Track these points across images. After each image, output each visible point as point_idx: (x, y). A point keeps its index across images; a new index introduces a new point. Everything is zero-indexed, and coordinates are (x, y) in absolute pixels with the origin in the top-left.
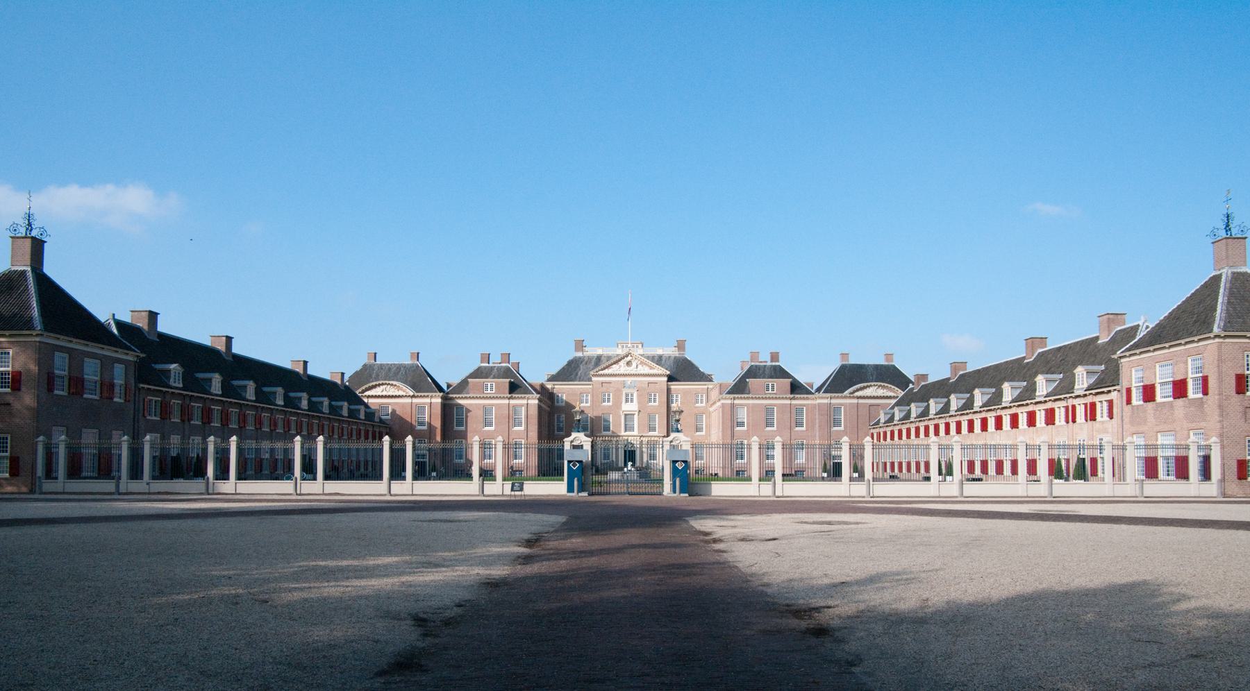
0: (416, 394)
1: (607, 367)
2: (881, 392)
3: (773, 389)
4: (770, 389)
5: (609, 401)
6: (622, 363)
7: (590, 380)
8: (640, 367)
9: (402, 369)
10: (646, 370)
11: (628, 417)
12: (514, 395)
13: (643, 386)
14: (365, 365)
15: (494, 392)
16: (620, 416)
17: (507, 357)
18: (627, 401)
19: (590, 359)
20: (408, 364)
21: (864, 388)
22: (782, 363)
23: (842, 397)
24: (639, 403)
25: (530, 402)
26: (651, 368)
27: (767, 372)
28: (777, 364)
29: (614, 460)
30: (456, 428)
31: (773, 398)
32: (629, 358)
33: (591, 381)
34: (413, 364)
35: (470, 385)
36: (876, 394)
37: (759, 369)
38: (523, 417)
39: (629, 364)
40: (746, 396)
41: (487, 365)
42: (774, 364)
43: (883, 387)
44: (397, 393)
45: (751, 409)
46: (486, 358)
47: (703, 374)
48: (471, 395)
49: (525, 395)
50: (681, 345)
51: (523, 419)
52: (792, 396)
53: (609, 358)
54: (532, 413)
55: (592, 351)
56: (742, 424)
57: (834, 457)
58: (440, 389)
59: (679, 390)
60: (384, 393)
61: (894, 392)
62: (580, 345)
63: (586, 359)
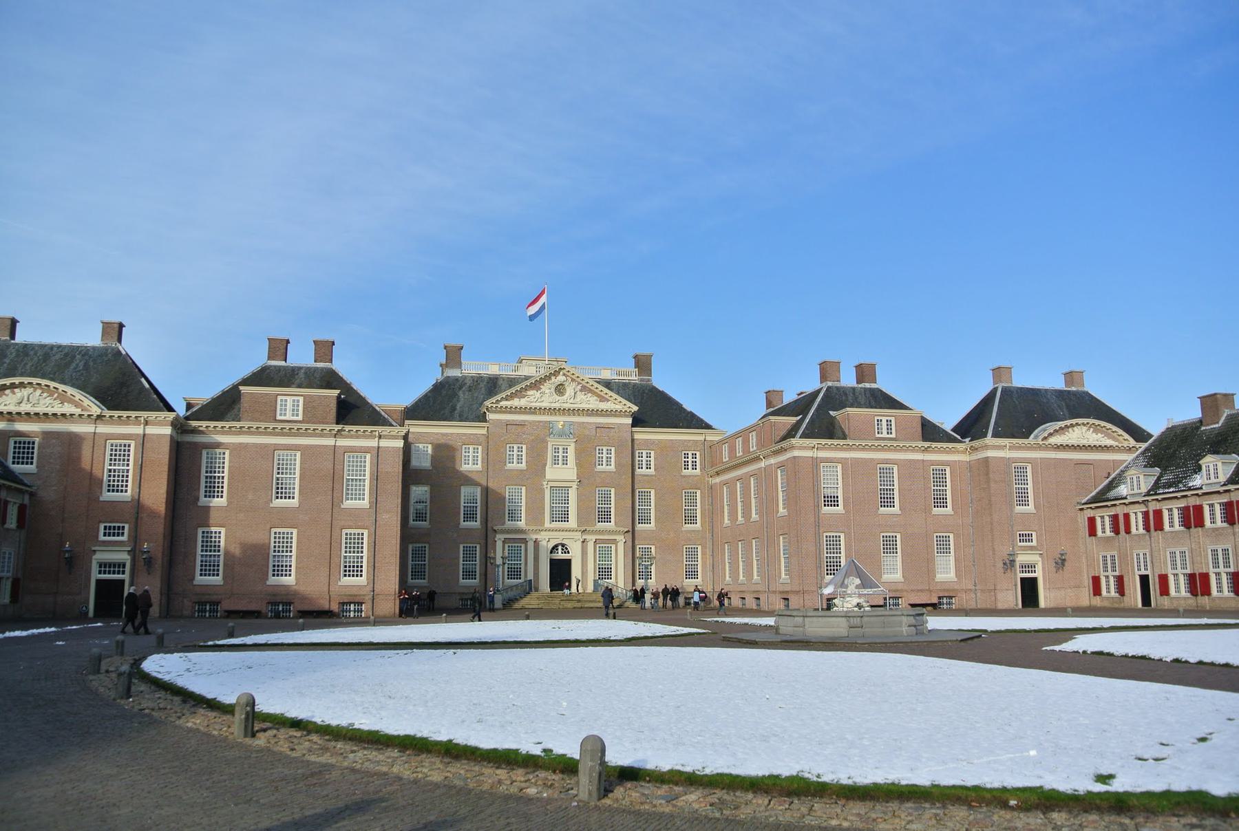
0: (108, 413)
1: (519, 394)
2: (1093, 438)
3: (889, 431)
4: (885, 431)
5: (519, 461)
6: (547, 388)
7: (482, 418)
8: (581, 396)
10: (592, 402)
11: (560, 491)
13: (587, 432)
15: (300, 418)
16: (542, 491)
17: (324, 349)
18: (555, 461)
19: (478, 380)
20: (94, 348)
22: (884, 383)
24: (579, 465)
25: (384, 443)
28: (874, 386)
30: (203, 501)
32: (561, 378)
33: (485, 421)
34: (106, 349)
35: (245, 403)
38: (368, 477)
39: (560, 389)
41: (282, 363)
42: (868, 385)
43: (1097, 429)
44: (58, 409)
46: (279, 347)
47: (692, 415)
50: (643, 364)
51: (367, 483)
52: (927, 444)
53: (512, 382)
55: (471, 367)
56: (832, 501)
59: (653, 442)
60: (25, 408)
61: (1114, 439)
62: (453, 355)
63: (468, 382)
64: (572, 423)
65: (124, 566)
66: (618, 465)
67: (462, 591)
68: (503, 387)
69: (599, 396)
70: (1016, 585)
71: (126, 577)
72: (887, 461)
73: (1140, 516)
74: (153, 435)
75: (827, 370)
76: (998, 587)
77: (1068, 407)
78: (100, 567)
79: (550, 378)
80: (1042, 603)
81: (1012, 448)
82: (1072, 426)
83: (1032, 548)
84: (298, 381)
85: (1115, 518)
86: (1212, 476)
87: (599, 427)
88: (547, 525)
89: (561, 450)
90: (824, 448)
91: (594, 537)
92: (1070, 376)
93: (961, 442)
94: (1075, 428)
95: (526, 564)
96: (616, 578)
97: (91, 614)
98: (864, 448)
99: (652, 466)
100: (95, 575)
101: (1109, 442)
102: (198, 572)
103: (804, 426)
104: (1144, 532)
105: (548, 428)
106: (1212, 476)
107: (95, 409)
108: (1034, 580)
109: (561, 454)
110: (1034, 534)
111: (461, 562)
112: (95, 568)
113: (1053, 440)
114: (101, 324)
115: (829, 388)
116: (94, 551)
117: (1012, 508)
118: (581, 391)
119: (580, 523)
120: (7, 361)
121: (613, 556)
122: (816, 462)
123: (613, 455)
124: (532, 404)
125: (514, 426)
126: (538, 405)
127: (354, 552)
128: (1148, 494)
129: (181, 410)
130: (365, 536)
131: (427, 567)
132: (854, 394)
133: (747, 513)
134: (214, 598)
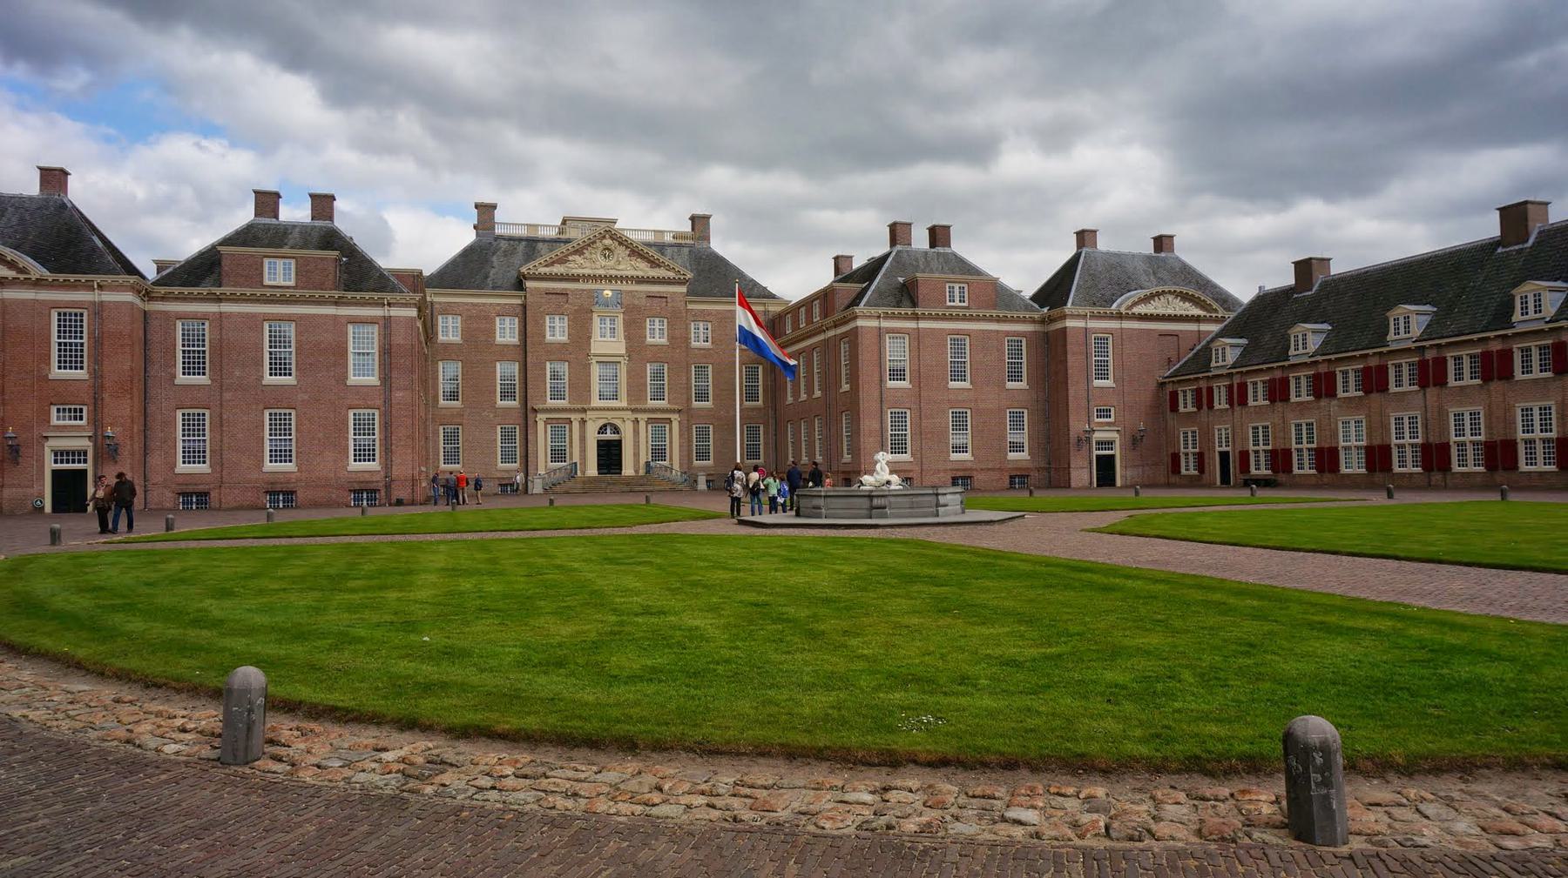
1: (562, 261)
4: (957, 299)
10: (643, 269)
12: (349, 295)
13: (636, 302)
15: (292, 283)
17: (323, 204)
20: (31, 199)
21: (1152, 297)
23: (1111, 317)
24: (628, 338)
25: (395, 312)
26: (654, 264)
28: (947, 250)
29: (576, 459)
30: (181, 379)
31: (965, 318)
36: (1170, 311)
40: (909, 311)
43: (1185, 297)
45: (917, 337)
46: (267, 201)
47: (755, 284)
48: (227, 290)
49: (380, 295)
57: (1102, 444)
58: (131, 269)
59: (709, 313)
65: (85, 453)
66: (671, 338)
67: (499, 475)
68: (543, 252)
69: (649, 261)
70: (1091, 463)
71: (89, 466)
72: (958, 332)
73: (1223, 390)
74: (110, 302)
75: (897, 233)
76: (1072, 466)
77: (1154, 273)
78: (56, 455)
79: (594, 242)
80: (1119, 483)
81: (1094, 317)
82: (1158, 294)
83: (1109, 424)
84: (291, 242)
85: (1198, 392)
86: (1300, 346)
88: (596, 402)
90: (887, 317)
91: (643, 417)
92: (1162, 243)
93: (1038, 311)
94: (1161, 297)
95: (571, 446)
96: (671, 459)
97: (48, 508)
98: (931, 318)
99: (710, 339)
100: (50, 465)
101: (1197, 312)
102: (180, 459)
103: (869, 293)
104: (1227, 406)
105: (594, 297)
106: (1300, 346)
107: (37, 270)
108: (1113, 457)
110: (1112, 409)
111: (499, 444)
112: (49, 458)
113: (1136, 310)
114: (39, 171)
115: (899, 252)
116: (46, 437)
117: (1088, 381)
118: (629, 255)
119: (629, 402)
121: (667, 436)
122: (880, 332)
123: (665, 327)
124: (574, 271)
125: (554, 296)
126: (580, 271)
127: (364, 434)
128: (1233, 367)
129: (151, 273)
130: (377, 417)
131: (461, 450)
133: (810, 391)
134: (201, 488)
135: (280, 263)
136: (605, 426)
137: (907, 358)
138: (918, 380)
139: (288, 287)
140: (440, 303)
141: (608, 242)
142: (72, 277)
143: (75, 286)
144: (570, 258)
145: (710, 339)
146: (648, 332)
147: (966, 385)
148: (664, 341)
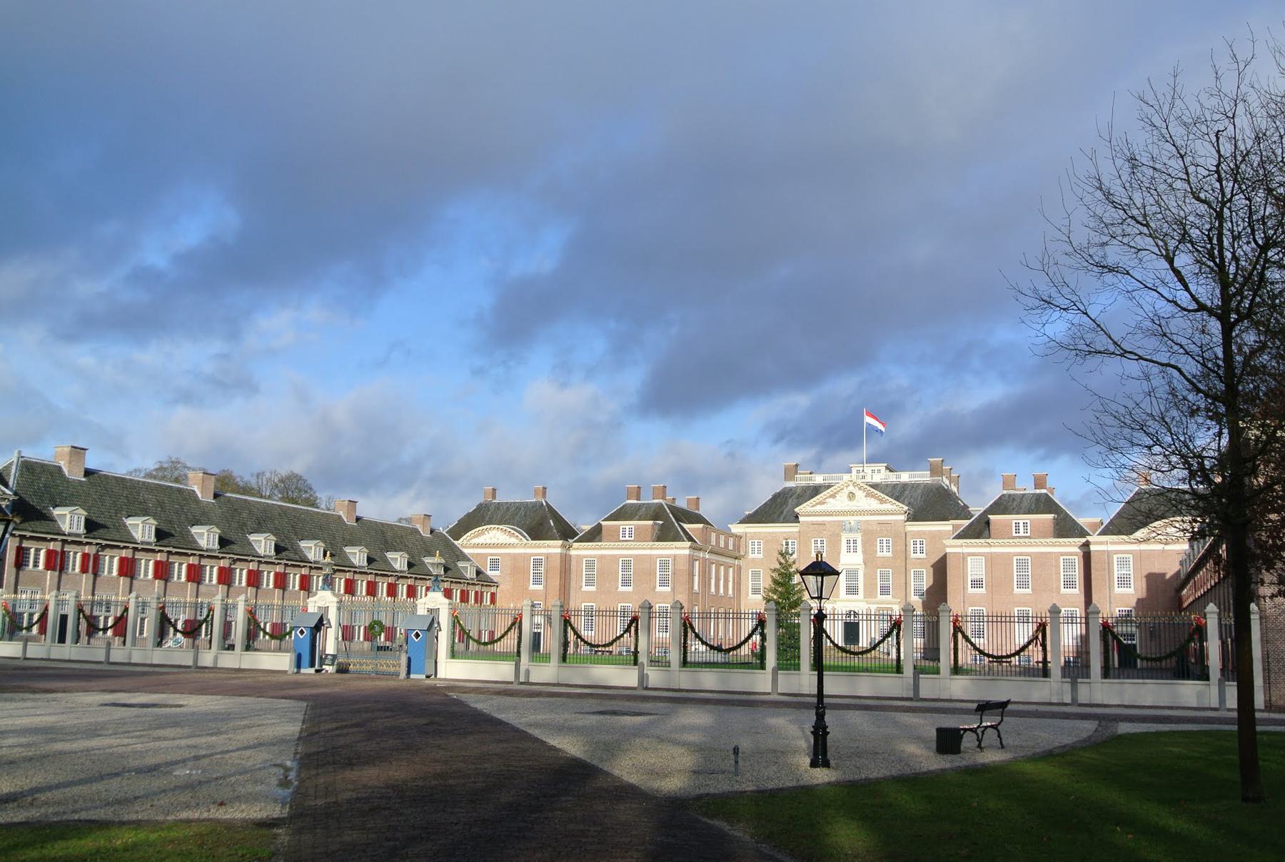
0: (531, 542)
7: (796, 518)
9: (523, 508)
13: (870, 528)
14: (481, 504)
15: (632, 539)
24: (864, 552)
26: (882, 501)
27: (1025, 504)
37: (1014, 500)
41: (635, 502)
42: (1038, 491)
45: (991, 560)
54: (682, 568)
56: (977, 583)
60: (494, 541)
63: (799, 491)
64: (859, 522)
87: (880, 523)
89: (852, 542)
108: (1135, 645)
109: (852, 545)
118: (866, 496)
120: (489, 513)
132: (1021, 499)
135: (627, 527)
136: (850, 611)
137: (984, 573)
138: (991, 588)
139: (630, 541)
140: (750, 533)
141: (851, 488)
142: (538, 542)
143: (539, 547)
144: (827, 500)
145: (924, 551)
146: (878, 547)
147: (1029, 591)
148: (890, 554)
